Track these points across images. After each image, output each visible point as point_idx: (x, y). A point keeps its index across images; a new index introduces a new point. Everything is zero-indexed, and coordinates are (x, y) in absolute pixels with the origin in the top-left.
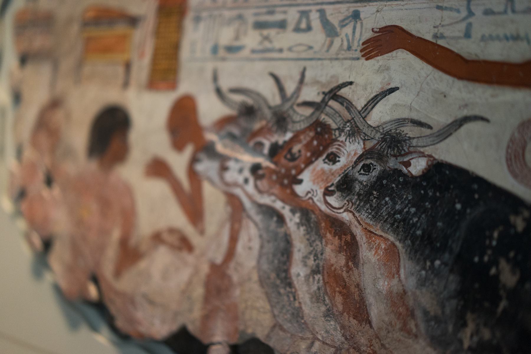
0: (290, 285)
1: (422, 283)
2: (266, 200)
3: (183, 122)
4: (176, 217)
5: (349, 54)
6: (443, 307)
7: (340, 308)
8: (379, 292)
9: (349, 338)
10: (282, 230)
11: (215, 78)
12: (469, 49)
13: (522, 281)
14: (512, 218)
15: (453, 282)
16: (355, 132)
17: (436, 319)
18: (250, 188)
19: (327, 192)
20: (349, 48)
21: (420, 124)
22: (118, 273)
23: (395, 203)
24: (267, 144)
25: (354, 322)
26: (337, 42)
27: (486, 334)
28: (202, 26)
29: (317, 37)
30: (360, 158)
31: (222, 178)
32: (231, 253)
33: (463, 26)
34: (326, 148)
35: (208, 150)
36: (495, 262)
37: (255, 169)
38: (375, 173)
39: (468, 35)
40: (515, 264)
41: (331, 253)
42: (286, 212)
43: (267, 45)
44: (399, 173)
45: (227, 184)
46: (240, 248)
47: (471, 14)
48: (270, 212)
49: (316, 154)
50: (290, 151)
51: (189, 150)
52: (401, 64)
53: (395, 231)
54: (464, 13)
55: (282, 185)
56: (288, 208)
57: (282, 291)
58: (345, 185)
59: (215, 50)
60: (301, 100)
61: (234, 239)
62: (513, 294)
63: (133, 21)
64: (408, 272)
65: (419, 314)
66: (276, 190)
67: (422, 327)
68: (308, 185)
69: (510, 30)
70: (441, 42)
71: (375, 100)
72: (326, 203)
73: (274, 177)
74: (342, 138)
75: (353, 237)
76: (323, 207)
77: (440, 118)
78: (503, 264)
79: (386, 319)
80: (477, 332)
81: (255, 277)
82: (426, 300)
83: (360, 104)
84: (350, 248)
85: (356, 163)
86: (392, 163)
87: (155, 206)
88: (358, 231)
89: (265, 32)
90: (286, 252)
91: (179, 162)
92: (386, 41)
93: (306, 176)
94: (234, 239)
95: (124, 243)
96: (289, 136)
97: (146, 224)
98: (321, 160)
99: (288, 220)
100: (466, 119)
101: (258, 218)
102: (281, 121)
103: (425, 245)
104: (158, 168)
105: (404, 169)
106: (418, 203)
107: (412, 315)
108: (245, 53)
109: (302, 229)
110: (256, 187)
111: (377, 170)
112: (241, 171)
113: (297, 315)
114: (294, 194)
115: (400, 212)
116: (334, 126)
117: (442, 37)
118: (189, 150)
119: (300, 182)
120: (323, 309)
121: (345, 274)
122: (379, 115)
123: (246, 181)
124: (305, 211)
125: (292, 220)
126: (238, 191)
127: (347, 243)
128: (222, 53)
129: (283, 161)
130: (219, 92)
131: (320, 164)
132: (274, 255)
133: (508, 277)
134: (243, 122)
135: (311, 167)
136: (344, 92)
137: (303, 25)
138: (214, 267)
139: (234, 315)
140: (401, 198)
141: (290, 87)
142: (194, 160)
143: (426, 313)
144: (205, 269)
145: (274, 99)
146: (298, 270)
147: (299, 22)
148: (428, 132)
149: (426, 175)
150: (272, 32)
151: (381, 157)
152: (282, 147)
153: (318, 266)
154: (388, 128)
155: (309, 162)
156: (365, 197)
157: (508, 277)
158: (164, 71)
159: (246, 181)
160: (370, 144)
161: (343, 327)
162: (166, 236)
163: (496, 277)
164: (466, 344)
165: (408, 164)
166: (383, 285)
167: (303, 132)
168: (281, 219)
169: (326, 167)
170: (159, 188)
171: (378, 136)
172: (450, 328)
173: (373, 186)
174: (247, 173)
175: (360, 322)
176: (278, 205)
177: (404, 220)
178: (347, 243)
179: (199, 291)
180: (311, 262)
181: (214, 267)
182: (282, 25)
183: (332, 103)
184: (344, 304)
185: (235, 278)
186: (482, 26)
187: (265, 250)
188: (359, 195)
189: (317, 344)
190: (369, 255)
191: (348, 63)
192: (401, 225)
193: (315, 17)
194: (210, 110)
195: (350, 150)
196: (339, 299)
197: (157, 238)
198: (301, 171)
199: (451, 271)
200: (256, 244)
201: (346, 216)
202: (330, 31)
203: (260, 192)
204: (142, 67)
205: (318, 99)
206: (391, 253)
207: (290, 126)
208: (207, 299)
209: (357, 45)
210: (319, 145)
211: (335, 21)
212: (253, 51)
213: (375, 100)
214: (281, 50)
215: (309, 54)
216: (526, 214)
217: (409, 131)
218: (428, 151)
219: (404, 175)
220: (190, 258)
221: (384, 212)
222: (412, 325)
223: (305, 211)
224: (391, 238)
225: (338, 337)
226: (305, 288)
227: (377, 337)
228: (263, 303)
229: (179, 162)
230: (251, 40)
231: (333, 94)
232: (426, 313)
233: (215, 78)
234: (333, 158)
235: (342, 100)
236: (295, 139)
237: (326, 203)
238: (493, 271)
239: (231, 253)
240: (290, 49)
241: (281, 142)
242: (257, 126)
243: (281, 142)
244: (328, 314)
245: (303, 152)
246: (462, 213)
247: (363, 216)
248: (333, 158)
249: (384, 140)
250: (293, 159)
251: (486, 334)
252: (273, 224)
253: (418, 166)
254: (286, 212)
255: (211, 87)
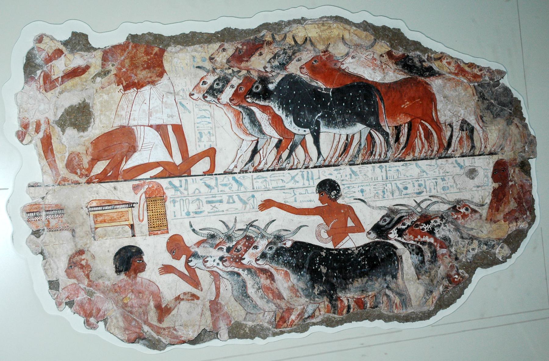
0: (249, 297)
1: (299, 280)
2: (230, 269)
3: (176, 246)
4: (187, 288)
5: (254, 210)
6: (307, 285)
7: (272, 298)
8: (285, 288)
9: (278, 306)
10: (241, 278)
11: (191, 226)
12: (297, 205)
13: (328, 270)
14: (321, 253)
15: (308, 277)
16: (263, 237)
17: (306, 289)
18: (221, 266)
19: (257, 260)
20: (253, 208)
21: (287, 230)
22: (160, 320)
23: (284, 258)
24: (225, 248)
25: (278, 301)
26: (248, 206)
27: (321, 288)
28: (177, 204)
29: (239, 205)
30: (267, 245)
31: (205, 266)
32: (218, 295)
33: (293, 198)
34: (252, 245)
35: (195, 255)
36: (319, 267)
37: (221, 259)
38: (274, 249)
39: (296, 201)
40: (325, 265)
41: (264, 281)
42: (240, 271)
43: (216, 209)
44: (283, 247)
45: (208, 267)
46: (221, 290)
47: (295, 194)
48: (233, 273)
49: (248, 247)
50: (236, 248)
51: (184, 258)
52: (274, 211)
53: (286, 267)
54: (293, 194)
55: (236, 262)
56: (241, 270)
57: (246, 300)
58: (264, 256)
59: (188, 214)
60: (236, 229)
61: (218, 289)
62: (326, 274)
63: (131, 205)
64: (293, 278)
65: (300, 290)
66: (234, 264)
67: (302, 293)
68: (249, 258)
69: (308, 199)
70: (287, 204)
71: (268, 225)
72: (257, 264)
73: (232, 260)
74: (258, 240)
75: (271, 273)
76: (256, 266)
77: (293, 228)
78: (321, 266)
79: (290, 295)
80: (319, 288)
81: (233, 299)
82: (301, 285)
83: (262, 227)
84: (271, 277)
85: (266, 247)
86: (280, 245)
87: (171, 287)
88: (273, 271)
89: (213, 205)
90: (244, 286)
91: (180, 265)
92: (267, 204)
93: (246, 256)
94: (218, 289)
95: (158, 307)
96: (234, 243)
97: (168, 296)
98: (251, 249)
99: (242, 274)
100: (301, 227)
101: (228, 277)
102: (229, 238)
103: (297, 269)
104: (167, 269)
105: (284, 246)
106: (292, 256)
107: (298, 291)
108: (206, 213)
109: (249, 276)
110: (223, 265)
111: (275, 248)
112: (214, 261)
113: (255, 306)
114: (242, 264)
115: (286, 260)
116: (254, 236)
117: (287, 202)
118: (184, 258)
119: (244, 259)
120: (265, 300)
121: (271, 286)
122: (272, 229)
123: (218, 264)
124: (249, 270)
125: (244, 274)
126: (215, 269)
127: (269, 276)
128: (192, 215)
129: (234, 253)
130: (194, 230)
131: (251, 251)
132: (239, 289)
133: (324, 270)
134: (210, 241)
135: (247, 252)
136: (254, 224)
137: (231, 201)
138: (211, 302)
139: (227, 316)
140: (285, 255)
141: (231, 225)
142: (187, 262)
143: (302, 289)
144: (208, 304)
145: (224, 230)
146: (251, 291)
147: (229, 199)
148: (289, 232)
149: (292, 246)
150: (217, 204)
151: (275, 244)
152: (232, 248)
153: (259, 287)
154: (275, 234)
155: (246, 251)
156: (272, 258)
157: (324, 270)
158: (158, 225)
159: (218, 264)
160: (270, 240)
161: (274, 304)
162: (181, 297)
163: (321, 270)
164: (316, 293)
165: (285, 244)
166: (286, 285)
167: (241, 240)
168: (239, 275)
169: (254, 251)
170: (172, 277)
171: (272, 237)
172: (311, 290)
173: (274, 254)
174: (217, 261)
175: (281, 300)
176: (236, 270)
177: (288, 262)
178: (269, 276)
179: (208, 313)
180: (256, 286)
181: (211, 302)
182: (221, 201)
183: (250, 228)
184: (273, 296)
185: (223, 303)
186: (300, 198)
187: (234, 288)
188: (270, 258)
189: (266, 313)
190: (279, 277)
191: (254, 213)
192: (288, 264)
193: (236, 198)
194: (190, 239)
195: (262, 244)
196: (270, 295)
197: (178, 299)
198: (244, 255)
199: (307, 274)
200: (229, 287)
201: (267, 267)
202: (245, 203)
203: (226, 267)
204: (142, 226)
205: (245, 227)
206: (286, 274)
207: (234, 239)
208: (212, 316)
209: (256, 207)
210: (249, 244)
211: (245, 199)
212: (209, 213)
213: (268, 225)
214: (223, 211)
215: (237, 211)
216: (325, 251)
217: (283, 233)
218: (291, 238)
219: (285, 248)
220: (199, 302)
221: (280, 261)
222: (298, 294)
223: (249, 270)
224: (285, 269)
225: (274, 307)
226: (255, 296)
227: (288, 302)
228: (239, 307)
229: (180, 265)
230: (207, 208)
231: (251, 225)
232: (302, 289)
233: (191, 226)
234: (256, 248)
235: (255, 227)
236: (238, 243)
237: (257, 264)
238: (319, 270)
239: (218, 295)
240: (227, 210)
241: (231, 246)
242: (218, 242)
243: (231, 246)
244: (268, 302)
245: (242, 248)
246: (307, 255)
247: (274, 265)
248: (256, 248)
249: (275, 238)
250: (238, 251)
251: (321, 288)
252: (235, 277)
253: (289, 244)
254: (240, 271)
255: (190, 229)
